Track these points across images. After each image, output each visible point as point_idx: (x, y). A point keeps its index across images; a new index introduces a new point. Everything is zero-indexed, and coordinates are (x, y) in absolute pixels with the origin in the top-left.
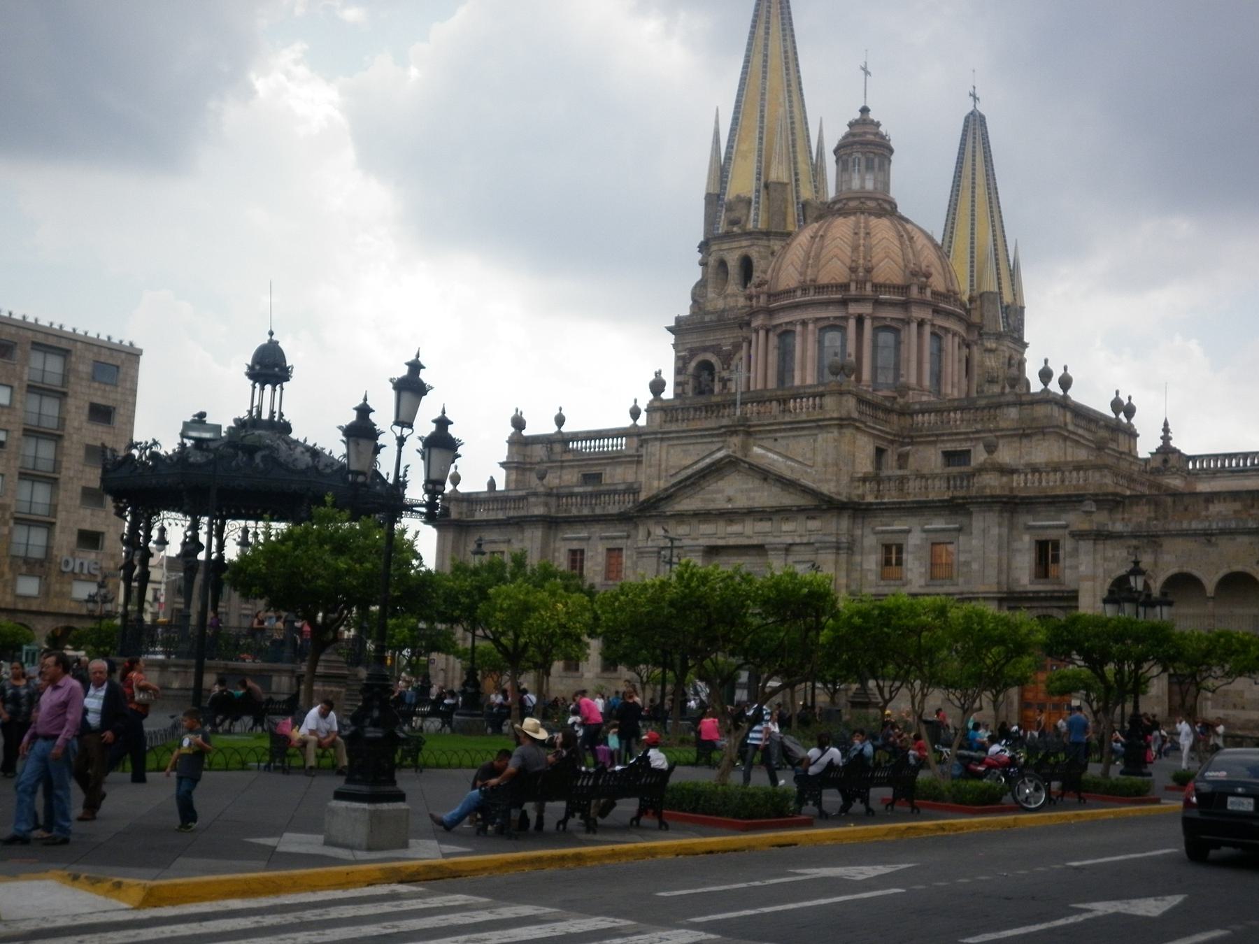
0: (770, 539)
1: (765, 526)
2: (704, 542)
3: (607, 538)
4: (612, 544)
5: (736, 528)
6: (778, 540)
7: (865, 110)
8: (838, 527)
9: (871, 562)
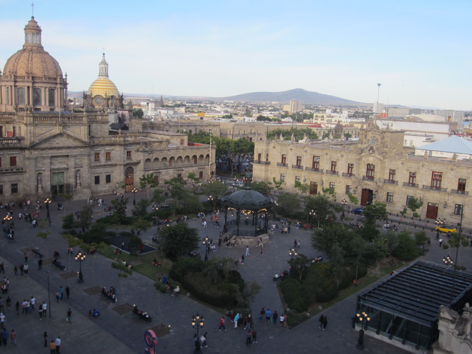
0: (69, 154)
1: (68, 150)
2: (50, 155)
3: (11, 154)
4: (12, 156)
5: (60, 151)
6: (72, 154)
7: (33, 17)
8: (87, 150)
9: (93, 158)
